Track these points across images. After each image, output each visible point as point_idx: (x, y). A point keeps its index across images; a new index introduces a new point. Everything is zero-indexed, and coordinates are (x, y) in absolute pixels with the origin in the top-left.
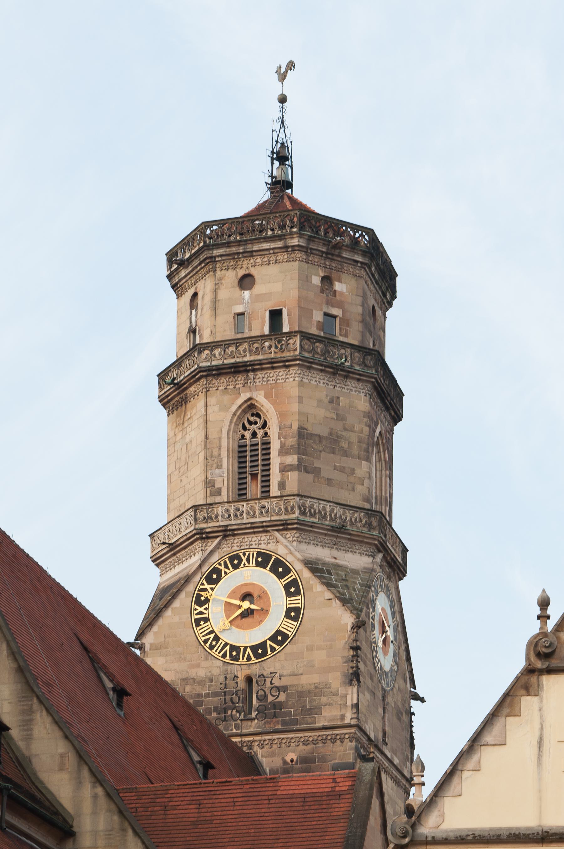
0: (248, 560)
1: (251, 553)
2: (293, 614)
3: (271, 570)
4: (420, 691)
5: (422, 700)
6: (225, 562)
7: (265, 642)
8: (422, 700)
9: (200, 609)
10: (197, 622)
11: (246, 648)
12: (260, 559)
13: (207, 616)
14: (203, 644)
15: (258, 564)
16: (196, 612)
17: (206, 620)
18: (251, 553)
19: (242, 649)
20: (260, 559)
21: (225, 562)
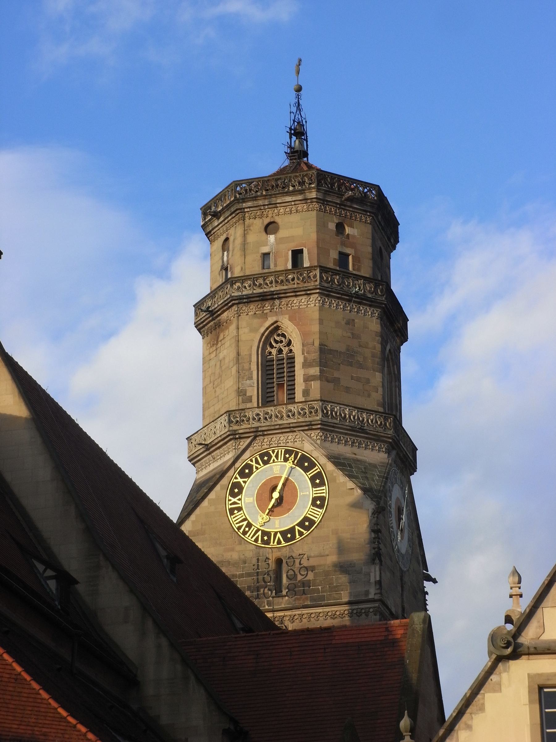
0: (277, 457)
1: (280, 450)
2: (318, 502)
4: (432, 572)
5: (435, 581)
6: (256, 459)
7: (294, 527)
8: (435, 581)
10: (232, 511)
13: (240, 505)
14: (237, 530)
16: (230, 502)
17: (240, 509)
18: (280, 450)
19: (273, 534)
21: (256, 459)
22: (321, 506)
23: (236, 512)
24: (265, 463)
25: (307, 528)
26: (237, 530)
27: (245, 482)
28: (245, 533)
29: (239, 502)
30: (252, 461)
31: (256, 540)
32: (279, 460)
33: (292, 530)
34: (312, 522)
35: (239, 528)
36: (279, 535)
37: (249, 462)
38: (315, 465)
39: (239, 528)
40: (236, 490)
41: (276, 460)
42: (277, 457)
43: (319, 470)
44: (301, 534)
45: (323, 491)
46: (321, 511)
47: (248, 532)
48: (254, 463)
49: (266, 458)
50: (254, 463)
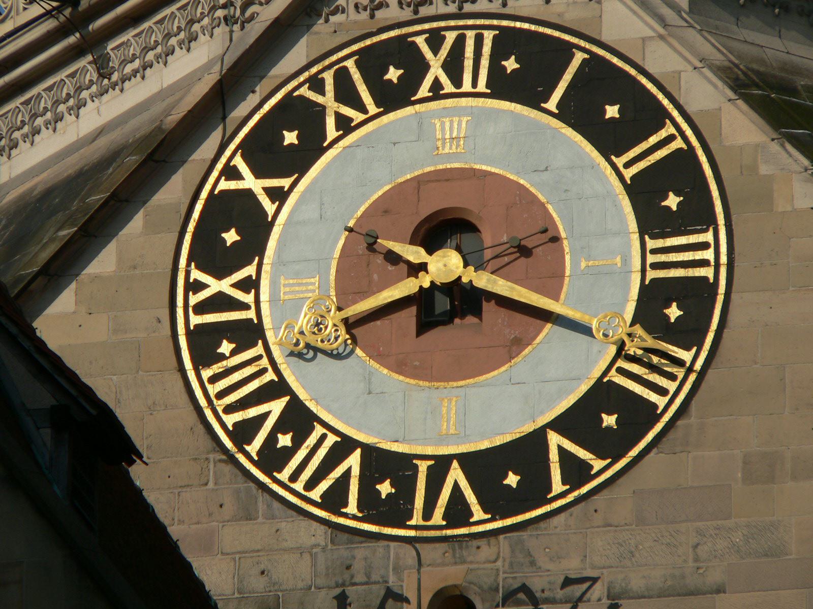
0: (453, 67)
1: (470, 35)
3: (564, 114)
6: (342, 77)
7: (537, 439)
9: (215, 286)
10: (204, 344)
11: (441, 466)
12: (511, 64)
13: (251, 314)
14: (229, 444)
15: (501, 86)
16: (194, 299)
19: (423, 466)
20: (511, 64)
21: (342, 77)
22: (688, 333)
23: (226, 347)
24: (392, 98)
25: (610, 446)
26: (229, 444)
27: (278, 196)
28: (272, 458)
29: (249, 298)
30: (317, 84)
31: (335, 499)
32: (467, 86)
33: (528, 451)
34: (638, 415)
35: (243, 433)
36: (456, 474)
37: (305, 91)
38: (660, 117)
39: (243, 433)
40: (231, 237)
41: (449, 88)
42: (453, 67)
43: (678, 144)
44: (576, 472)
45: (702, 253)
46: (686, 356)
47: (289, 453)
48: (328, 99)
49: (393, 74)
50: (328, 99)
